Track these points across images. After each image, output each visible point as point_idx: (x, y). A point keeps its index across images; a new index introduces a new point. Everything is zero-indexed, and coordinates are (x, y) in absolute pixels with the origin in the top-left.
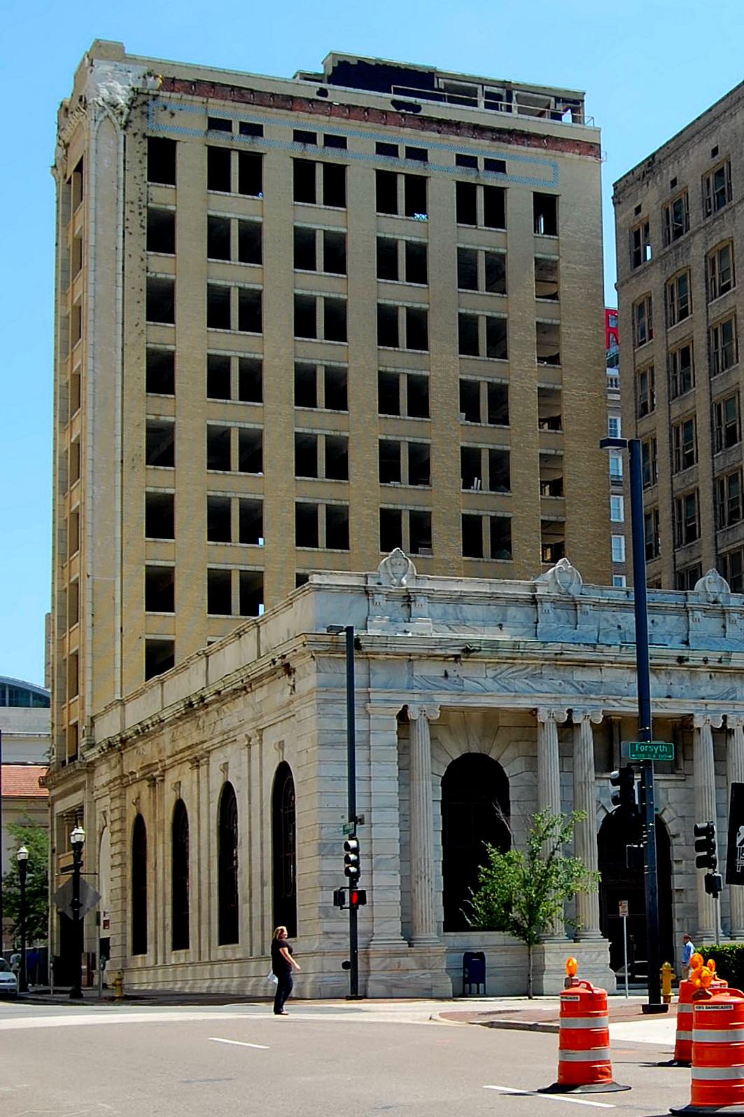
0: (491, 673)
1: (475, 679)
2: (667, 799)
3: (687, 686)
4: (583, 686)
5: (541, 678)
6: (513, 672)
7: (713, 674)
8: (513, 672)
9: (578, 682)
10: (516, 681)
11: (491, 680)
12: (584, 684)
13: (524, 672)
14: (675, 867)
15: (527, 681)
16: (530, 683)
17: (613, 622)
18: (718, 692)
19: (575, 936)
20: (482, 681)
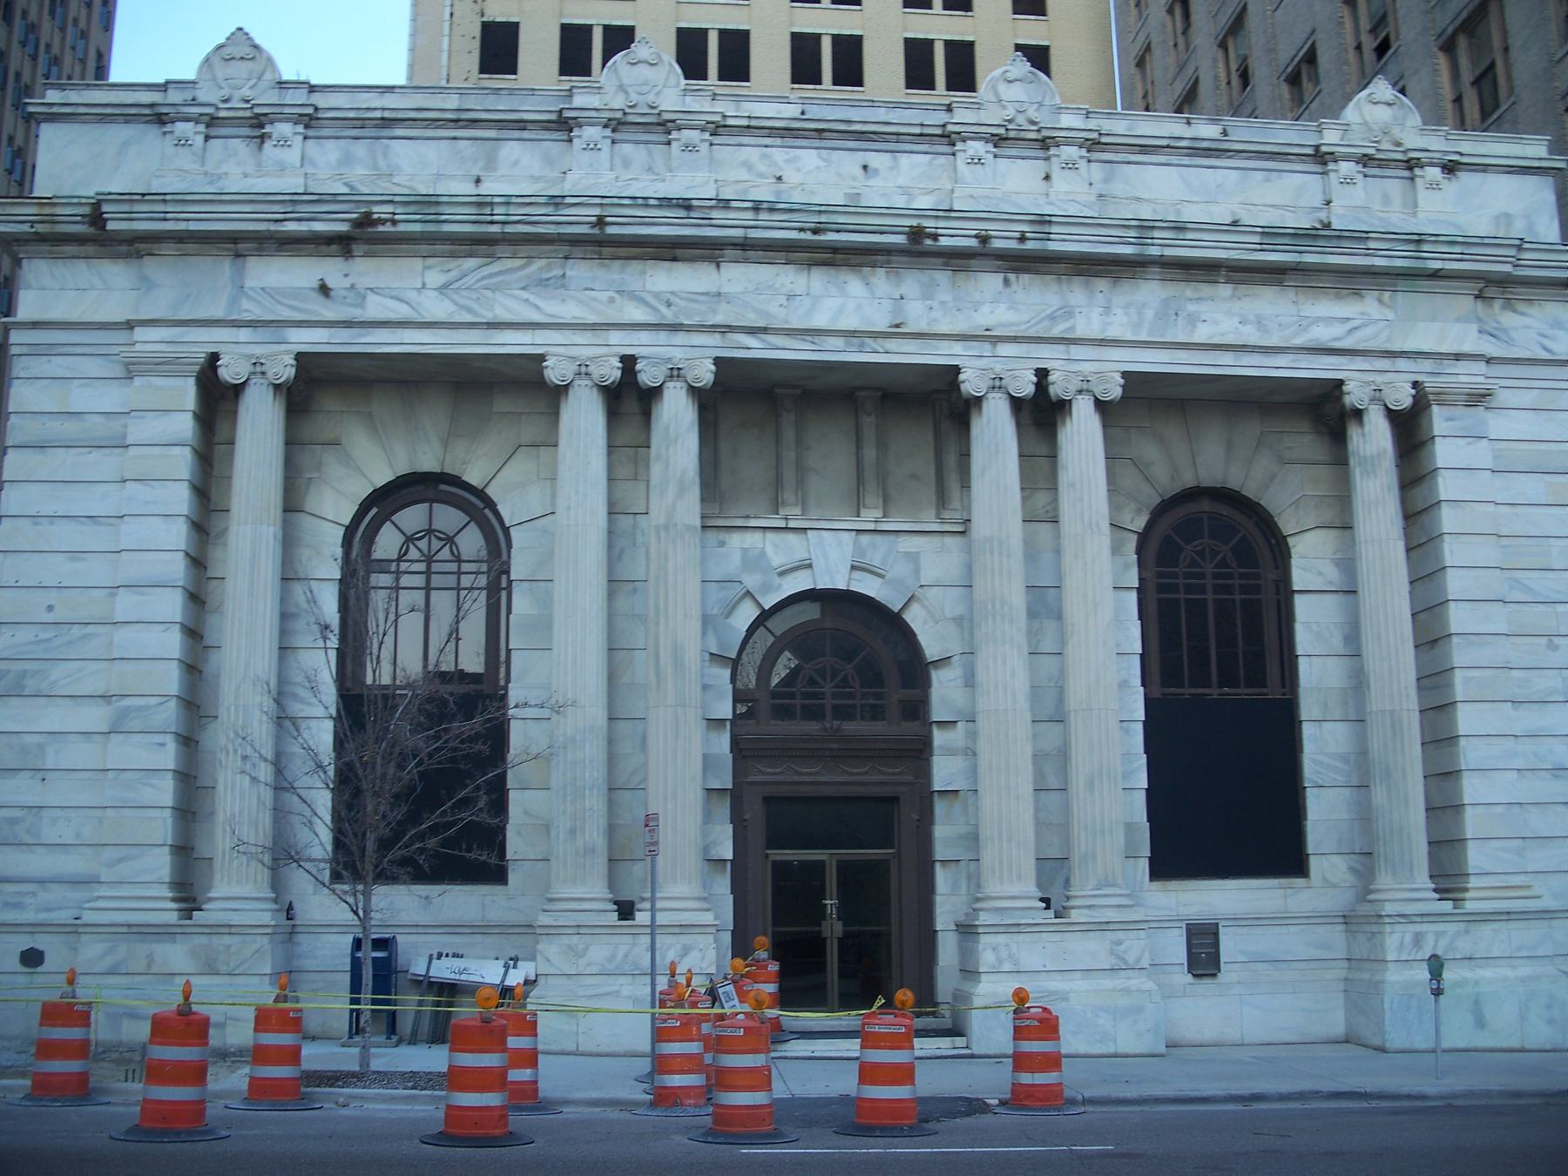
0: (435, 278)
1: (394, 293)
2: (918, 578)
3: (943, 303)
4: (669, 304)
5: (563, 286)
6: (491, 276)
7: (1012, 276)
8: (491, 276)
9: (657, 295)
10: (498, 296)
11: (435, 293)
12: (673, 299)
13: (520, 274)
14: (939, 738)
15: (524, 294)
16: (532, 299)
17: (762, 168)
18: (1026, 317)
19: (1019, 878)
20: (413, 295)
